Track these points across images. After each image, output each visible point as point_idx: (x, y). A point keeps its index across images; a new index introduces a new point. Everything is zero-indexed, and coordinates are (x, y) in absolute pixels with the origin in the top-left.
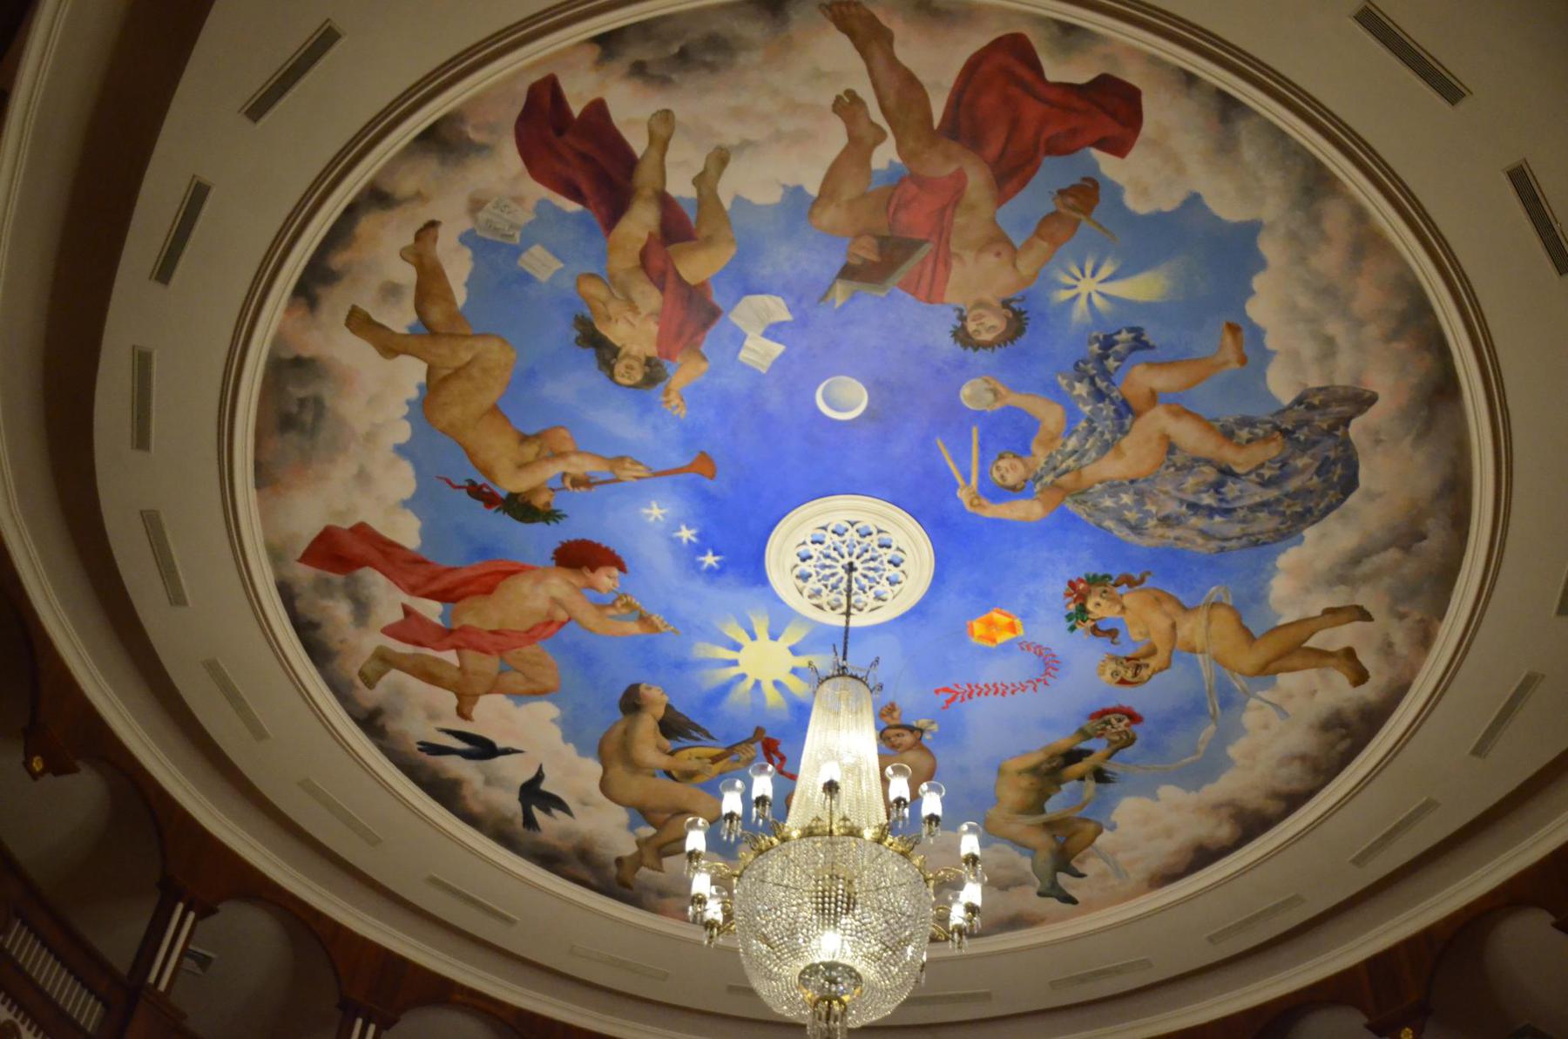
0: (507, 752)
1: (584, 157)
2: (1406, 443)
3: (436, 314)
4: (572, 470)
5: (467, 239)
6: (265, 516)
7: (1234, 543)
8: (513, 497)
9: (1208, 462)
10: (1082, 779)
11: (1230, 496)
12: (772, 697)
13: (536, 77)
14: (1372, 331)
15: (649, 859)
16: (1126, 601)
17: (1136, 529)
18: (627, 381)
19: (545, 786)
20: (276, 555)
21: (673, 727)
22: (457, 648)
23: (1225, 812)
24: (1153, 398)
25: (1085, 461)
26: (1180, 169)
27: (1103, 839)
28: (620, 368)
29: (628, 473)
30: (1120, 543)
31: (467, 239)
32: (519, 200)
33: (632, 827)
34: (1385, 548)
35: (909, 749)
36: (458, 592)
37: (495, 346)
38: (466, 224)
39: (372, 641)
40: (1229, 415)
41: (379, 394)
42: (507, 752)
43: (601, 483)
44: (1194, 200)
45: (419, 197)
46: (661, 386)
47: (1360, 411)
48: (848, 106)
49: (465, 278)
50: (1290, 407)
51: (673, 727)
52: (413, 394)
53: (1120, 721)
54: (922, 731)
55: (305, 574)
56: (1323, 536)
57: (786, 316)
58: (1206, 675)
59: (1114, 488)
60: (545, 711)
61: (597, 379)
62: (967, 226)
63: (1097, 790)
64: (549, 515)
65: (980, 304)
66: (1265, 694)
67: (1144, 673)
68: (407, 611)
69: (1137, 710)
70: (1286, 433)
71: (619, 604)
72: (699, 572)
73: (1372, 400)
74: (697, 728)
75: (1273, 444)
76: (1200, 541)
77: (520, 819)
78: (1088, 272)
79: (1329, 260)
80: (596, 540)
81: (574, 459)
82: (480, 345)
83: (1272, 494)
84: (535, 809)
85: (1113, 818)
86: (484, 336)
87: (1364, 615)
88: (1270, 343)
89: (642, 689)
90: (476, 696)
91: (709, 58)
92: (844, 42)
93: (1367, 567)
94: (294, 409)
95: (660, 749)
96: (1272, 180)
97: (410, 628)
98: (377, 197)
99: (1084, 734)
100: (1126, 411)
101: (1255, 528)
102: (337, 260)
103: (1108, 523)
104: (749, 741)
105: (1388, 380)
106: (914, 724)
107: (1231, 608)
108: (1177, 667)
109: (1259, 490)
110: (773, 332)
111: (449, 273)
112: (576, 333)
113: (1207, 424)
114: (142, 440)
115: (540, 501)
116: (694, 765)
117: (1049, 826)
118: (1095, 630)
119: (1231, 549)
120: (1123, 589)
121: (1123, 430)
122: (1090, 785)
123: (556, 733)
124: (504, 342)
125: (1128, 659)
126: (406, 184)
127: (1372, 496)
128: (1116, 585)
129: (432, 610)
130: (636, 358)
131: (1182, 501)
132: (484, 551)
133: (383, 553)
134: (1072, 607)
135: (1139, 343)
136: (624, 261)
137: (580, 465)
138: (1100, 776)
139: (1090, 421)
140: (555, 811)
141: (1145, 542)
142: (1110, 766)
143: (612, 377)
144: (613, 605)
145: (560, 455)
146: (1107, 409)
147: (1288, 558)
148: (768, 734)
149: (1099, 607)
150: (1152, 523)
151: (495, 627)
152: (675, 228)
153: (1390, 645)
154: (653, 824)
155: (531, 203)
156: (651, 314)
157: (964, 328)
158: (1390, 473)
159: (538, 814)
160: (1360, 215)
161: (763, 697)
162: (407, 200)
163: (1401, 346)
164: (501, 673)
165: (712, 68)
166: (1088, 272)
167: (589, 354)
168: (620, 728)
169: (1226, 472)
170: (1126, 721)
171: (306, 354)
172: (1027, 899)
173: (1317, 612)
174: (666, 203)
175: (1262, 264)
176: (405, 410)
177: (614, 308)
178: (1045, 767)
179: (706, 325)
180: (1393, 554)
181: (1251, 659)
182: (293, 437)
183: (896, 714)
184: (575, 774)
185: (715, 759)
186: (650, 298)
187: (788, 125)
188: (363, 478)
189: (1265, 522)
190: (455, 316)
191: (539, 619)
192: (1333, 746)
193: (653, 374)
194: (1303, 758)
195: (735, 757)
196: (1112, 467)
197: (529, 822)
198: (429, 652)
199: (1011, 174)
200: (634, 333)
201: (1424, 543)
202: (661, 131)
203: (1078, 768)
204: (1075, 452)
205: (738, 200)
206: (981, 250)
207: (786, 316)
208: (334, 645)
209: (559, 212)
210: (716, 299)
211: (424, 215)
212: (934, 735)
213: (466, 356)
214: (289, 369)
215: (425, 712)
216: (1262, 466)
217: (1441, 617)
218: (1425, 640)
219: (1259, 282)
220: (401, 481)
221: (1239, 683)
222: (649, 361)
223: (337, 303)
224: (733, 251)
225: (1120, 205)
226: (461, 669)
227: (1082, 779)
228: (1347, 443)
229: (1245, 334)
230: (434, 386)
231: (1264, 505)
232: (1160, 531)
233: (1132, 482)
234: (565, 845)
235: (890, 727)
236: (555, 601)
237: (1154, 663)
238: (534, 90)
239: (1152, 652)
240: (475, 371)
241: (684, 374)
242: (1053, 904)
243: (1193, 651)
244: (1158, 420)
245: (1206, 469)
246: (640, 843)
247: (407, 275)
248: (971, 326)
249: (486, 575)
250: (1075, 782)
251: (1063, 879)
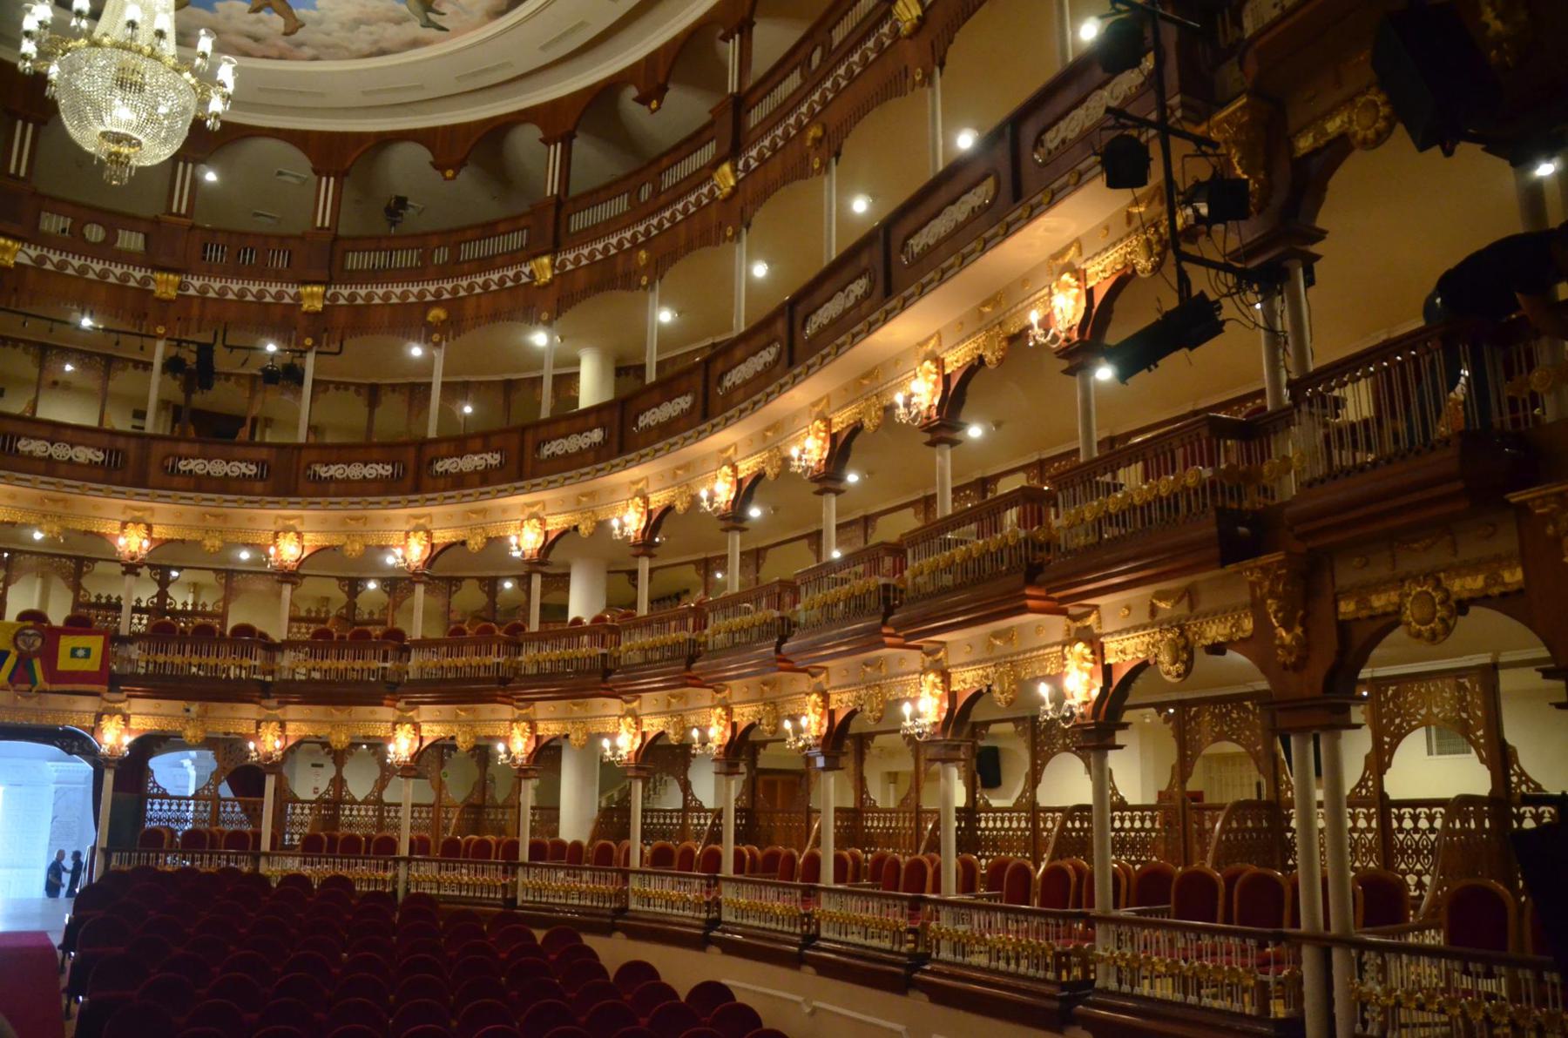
172: (415, 29)
242: (432, 32)
251: (432, 16)
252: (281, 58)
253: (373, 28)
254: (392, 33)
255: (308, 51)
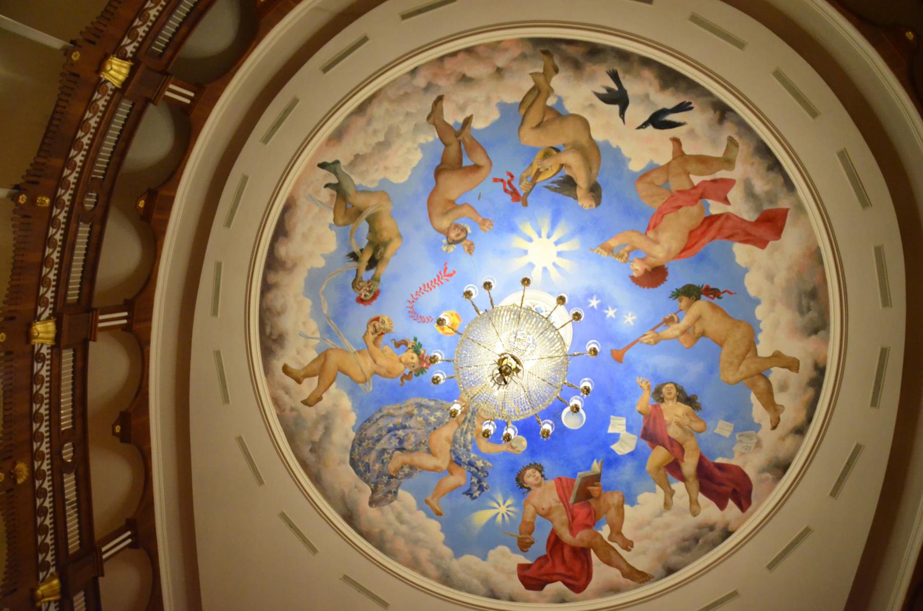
0: (644, 125)
1: (723, 485)
2: (346, 490)
3: (761, 384)
4: (676, 326)
5: (757, 427)
6: (811, 234)
7: (378, 416)
8: (698, 298)
9: (411, 451)
10: (362, 250)
11: (393, 438)
12: (528, 229)
13: (750, 509)
14: (390, 533)
15: (541, 79)
16: (402, 367)
17: (420, 406)
18: (668, 386)
19: (616, 108)
20: (800, 208)
21: (568, 184)
22: (695, 188)
23: (289, 265)
24: (450, 472)
25: (459, 430)
26: (496, 567)
27: (330, 217)
28: (674, 391)
29: (650, 335)
30: (422, 395)
31: (757, 427)
32: (742, 454)
33: (560, 100)
34: (321, 439)
35: (449, 229)
36: (705, 227)
37: (732, 379)
38: (760, 434)
39: (737, 173)
40: (417, 476)
41: (776, 331)
42: (644, 125)
43: (660, 325)
44: (484, 558)
45: (783, 439)
46: (653, 390)
47: (371, 498)
48: (628, 545)
49: (754, 409)
50: (397, 488)
51: (568, 184)
52: (760, 337)
53: (365, 295)
54: (449, 244)
55: (784, 203)
56: (347, 435)
57: (613, 447)
58: (346, 341)
59: (440, 423)
60: (636, 166)
61: (683, 381)
62: (560, 519)
63: (351, 247)
64: (677, 294)
65: (539, 485)
66: (317, 342)
67: (371, 329)
68: (726, 201)
69: (361, 305)
70: (391, 477)
71: (626, 255)
72: (596, 293)
73: (371, 504)
74: (555, 190)
75: (393, 469)
76: (391, 411)
77: (621, 75)
78: (506, 516)
79: (424, 554)
80: (651, 289)
81: (677, 333)
82: (738, 376)
83: (379, 447)
84: (616, 88)
85: (334, 233)
86: (737, 382)
87: (305, 402)
88: (422, 514)
89: (594, 205)
90: (674, 159)
91: (687, 543)
92: (640, 568)
93: (321, 428)
94: (812, 304)
95: (569, 167)
96: (462, 576)
97: (720, 189)
98: (800, 431)
99: (375, 279)
100: (457, 461)
101: (374, 428)
102: (811, 392)
103: (432, 403)
104: (527, 194)
105: (371, 515)
106: (455, 246)
107: (358, 382)
108: (360, 340)
109: (385, 447)
110: (615, 438)
111: (761, 407)
112: (698, 401)
113: (423, 469)
114: (879, 251)
115: (685, 300)
116: (547, 163)
117: (359, 212)
118: (405, 343)
119: (377, 412)
120: (407, 371)
121: (453, 451)
122: (356, 249)
123: (626, 152)
124: (728, 382)
125: (382, 334)
126: (790, 442)
127: (342, 462)
128: (411, 372)
129: (715, 208)
130: (669, 399)
131: (410, 428)
132: (702, 258)
133: (748, 234)
134: (422, 352)
135: (469, 493)
136: (690, 445)
137: (672, 331)
138: (354, 257)
139: (468, 450)
140: (604, 91)
141: (412, 401)
142: (353, 265)
143: (676, 385)
144: (628, 252)
145: (684, 332)
146: (464, 459)
147: (353, 418)
148: (520, 203)
149: (410, 357)
150: (416, 412)
151: (680, 210)
152: (674, 468)
153: (287, 393)
154: (551, 109)
155: (736, 455)
156: (670, 424)
157: (540, 472)
158: (344, 476)
159: (613, 86)
160: (424, 573)
161: (534, 228)
162: (787, 435)
163: (377, 530)
164: (667, 181)
165: (684, 540)
166: (506, 516)
167: (689, 393)
168: (594, 171)
169: (402, 449)
170: (362, 297)
171: (814, 337)
172: (342, 154)
173: (324, 396)
174: (682, 478)
175: (445, 543)
176: (761, 326)
177: (686, 421)
178: (382, 250)
179: (645, 429)
180: (316, 438)
181: (334, 358)
182: (809, 287)
183: (466, 248)
184: (605, 125)
185: (538, 173)
186: (673, 432)
187: (647, 529)
188: (770, 278)
189: (372, 432)
190: (753, 386)
191: (661, 226)
192: (272, 327)
193: (658, 395)
194: (279, 314)
195: (529, 179)
196: (447, 431)
197: (614, 76)
198: (708, 178)
199: (555, 542)
200: (674, 411)
201: (309, 448)
202: (695, 507)
203: (366, 257)
204: (466, 433)
205: (653, 491)
206: (550, 508)
207: (613, 447)
208: (757, 160)
209: (724, 456)
210: (645, 443)
211: (780, 430)
212: (442, 244)
213: (743, 368)
214: (818, 327)
215: (697, 132)
216: (391, 458)
217: (278, 415)
218: (276, 401)
219: (442, 536)
220: (753, 283)
221: (330, 343)
222: (662, 400)
223: (806, 371)
224: (647, 468)
225: (509, 546)
226: (687, 174)
227: (362, 250)
228: (367, 482)
229: (433, 513)
230: (752, 345)
231: (378, 440)
232: (410, 409)
233: (435, 429)
234: (590, 67)
235: (465, 238)
236: (657, 242)
237: (371, 337)
238: (749, 503)
239: (375, 342)
240: (736, 361)
241: (644, 401)
243: (359, 352)
244: (443, 461)
245: (410, 447)
246: (550, 91)
247: (779, 399)
248: (538, 474)
249: (696, 243)
250: (363, 247)
251: (333, 180)
252: (441, 59)
253: (374, 141)
254: (356, 143)
255: (420, 81)
